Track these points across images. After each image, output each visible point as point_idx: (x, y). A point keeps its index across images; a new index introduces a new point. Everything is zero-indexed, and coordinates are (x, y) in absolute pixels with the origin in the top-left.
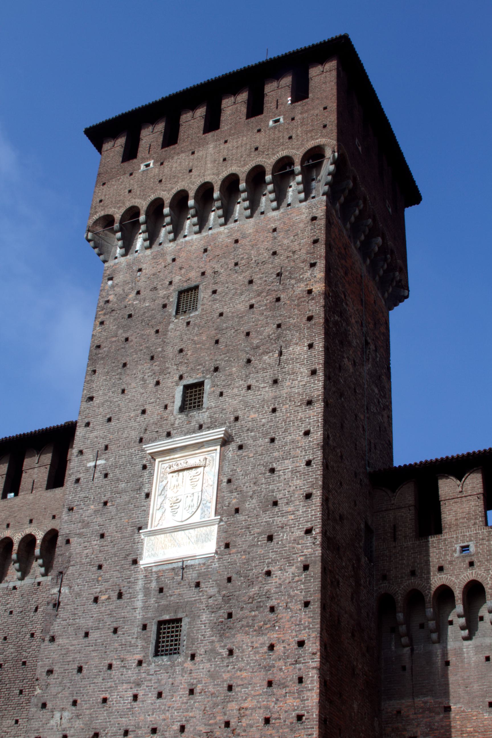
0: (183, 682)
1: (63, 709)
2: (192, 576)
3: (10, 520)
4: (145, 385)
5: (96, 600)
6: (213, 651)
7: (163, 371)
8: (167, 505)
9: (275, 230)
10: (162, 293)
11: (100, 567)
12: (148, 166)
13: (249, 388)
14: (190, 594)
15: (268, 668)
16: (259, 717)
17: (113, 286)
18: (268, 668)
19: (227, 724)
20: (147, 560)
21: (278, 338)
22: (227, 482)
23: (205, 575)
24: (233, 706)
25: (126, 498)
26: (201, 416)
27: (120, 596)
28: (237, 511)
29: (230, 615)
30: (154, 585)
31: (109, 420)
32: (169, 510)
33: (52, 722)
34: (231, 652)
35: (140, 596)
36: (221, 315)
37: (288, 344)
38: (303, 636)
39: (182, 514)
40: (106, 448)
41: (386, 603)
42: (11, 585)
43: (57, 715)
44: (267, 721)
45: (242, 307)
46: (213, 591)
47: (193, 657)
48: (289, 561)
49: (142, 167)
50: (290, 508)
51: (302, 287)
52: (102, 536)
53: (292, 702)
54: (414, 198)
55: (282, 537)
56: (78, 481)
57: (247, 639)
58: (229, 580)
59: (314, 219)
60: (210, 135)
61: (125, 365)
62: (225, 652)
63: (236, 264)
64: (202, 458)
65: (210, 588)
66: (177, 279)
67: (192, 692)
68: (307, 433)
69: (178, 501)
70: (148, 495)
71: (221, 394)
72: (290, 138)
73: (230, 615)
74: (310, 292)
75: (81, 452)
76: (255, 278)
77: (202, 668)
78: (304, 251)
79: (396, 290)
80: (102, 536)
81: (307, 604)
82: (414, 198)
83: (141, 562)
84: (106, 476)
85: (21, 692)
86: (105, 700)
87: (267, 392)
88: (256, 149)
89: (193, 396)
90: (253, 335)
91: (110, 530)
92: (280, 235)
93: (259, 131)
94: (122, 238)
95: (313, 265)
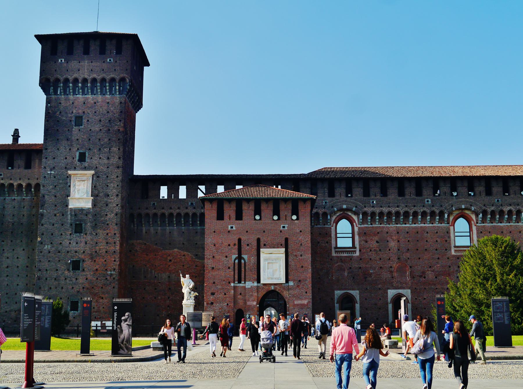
0: (83, 240)
1: (48, 245)
2: (85, 212)
3: (12, 177)
4: (65, 149)
5: (55, 215)
6: (92, 233)
7: (72, 145)
8: (76, 190)
9: (108, 103)
10: (70, 115)
11: (56, 206)
12: (62, 61)
13: (100, 158)
14: (85, 218)
15: (106, 239)
16: (104, 250)
17: (50, 107)
18: (106, 239)
19: (96, 252)
20: (70, 206)
21: (110, 143)
22: (94, 187)
23: (89, 213)
24: (97, 248)
25: (62, 186)
26: (86, 164)
27: (63, 215)
28: (97, 196)
29: (96, 225)
30: (73, 213)
31: (54, 158)
32: (77, 192)
33: (45, 248)
34: (96, 234)
35: (69, 216)
36: (91, 130)
37: (112, 146)
38: (116, 232)
39: (81, 194)
40: (54, 168)
41: (132, 216)
42: (13, 198)
43: (46, 246)
44: (106, 252)
45: (98, 129)
46: (91, 217)
47: (86, 234)
48: (112, 212)
49: (60, 61)
50: (113, 198)
51: (116, 128)
52: (55, 196)
53: (112, 248)
54: (148, 65)
55: (110, 205)
56: (45, 177)
57: (101, 231)
58: (96, 215)
59: (121, 103)
60: (86, 56)
61: (58, 140)
62: (95, 234)
63: (95, 112)
64: (85, 178)
65: (90, 216)
66: (74, 111)
67: (86, 243)
68: (117, 177)
69: (79, 190)
70: (70, 186)
71: (91, 158)
72: (115, 70)
73: (96, 225)
74: (119, 130)
75: (45, 168)
76: (102, 119)
77: (89, 238)
78: (117, 114)
79: (138, 105)
80: (55, 196)
81: (117, 224)
82: (148, 65)
83: (70, 207)
84: (55, 177)
85: (22, 232)
86: (61, 243)
87: (106, 161)
88: (103, 70)
89: (82, 158)
90: (101, 140)
91: (58, 195)
92: (110, 106)
93: (104, 62)
94: (54, 89)
95: (120, 121)
